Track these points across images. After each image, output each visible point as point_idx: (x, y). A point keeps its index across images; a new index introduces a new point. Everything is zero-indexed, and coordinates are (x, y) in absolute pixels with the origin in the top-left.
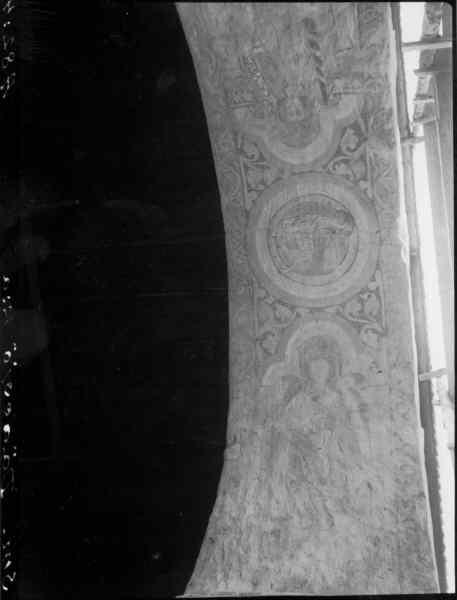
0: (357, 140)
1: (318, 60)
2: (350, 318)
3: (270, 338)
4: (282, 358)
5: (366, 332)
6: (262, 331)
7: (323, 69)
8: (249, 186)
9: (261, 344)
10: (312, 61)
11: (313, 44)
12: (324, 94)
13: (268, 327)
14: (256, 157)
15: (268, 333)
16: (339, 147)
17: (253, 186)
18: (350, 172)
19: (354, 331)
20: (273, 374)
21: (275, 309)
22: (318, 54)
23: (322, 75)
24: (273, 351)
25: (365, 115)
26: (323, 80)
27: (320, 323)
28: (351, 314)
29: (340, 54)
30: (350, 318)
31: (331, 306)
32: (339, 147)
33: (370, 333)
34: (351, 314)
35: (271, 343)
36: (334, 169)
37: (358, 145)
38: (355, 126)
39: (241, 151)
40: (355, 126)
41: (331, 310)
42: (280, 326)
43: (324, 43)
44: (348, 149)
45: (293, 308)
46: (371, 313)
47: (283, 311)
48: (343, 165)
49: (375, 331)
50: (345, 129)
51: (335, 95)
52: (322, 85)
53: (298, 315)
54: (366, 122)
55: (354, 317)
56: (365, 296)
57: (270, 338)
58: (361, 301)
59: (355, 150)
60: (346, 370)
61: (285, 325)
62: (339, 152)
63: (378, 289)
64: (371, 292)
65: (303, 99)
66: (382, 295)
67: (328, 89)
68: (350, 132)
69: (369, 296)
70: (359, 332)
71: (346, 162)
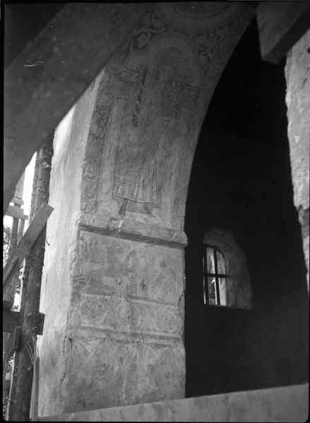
0: (139, 39)
1: (139, 100)
7: (138, 92)
8: (218, 40)
10: (142, 99)
11: (138, 110)
12: (144, 76)
14: (203, 54)
16: (151, 38)
17: (216, 38)
18: (153, 20)
22: (137, 102)
23: (141, 88)
25: (127, 52)
26: (141, 85)
29: (127, 97)
32: (151, 38)
36: (161, 26)
37: (140, 35)
38: (136, 47)
39: (209, 60)
40: (136, 47)
43: (131, 108)
44: (147, 34)
48: (155, 26)
50: (144, 47)
51: (139, 72)
52: (143, 82)
54: (128, 48)
59: (143, 33)
62: (153, 35)
65: (157, 79)
67: (141, 77)
68: (140, 45)
71: (152, 27)
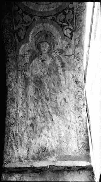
2: (60, 23)
3: (21, 31)
4: (27, 41)
5: (66, 30)
6: (16, 29)
9: (17, 34)
13: (19, 26)
15: (20, 28)
19: (61, 29)
20: (24, 49)
21: (23, 16)
24: (23, 38)
27: (45, 24)
28: (59, 20)
30: (60, 23)
31: (49, 16)
33: (68, 30)
34: (59, 20)
35: (22, 33)
41: (50, 18)
42: (25, 25)
45: (31, 16)
46: (69, 20)
47: (27, 18)
49: (70, 29)
53: (34, 20)
55: (61, 22)
56: (67, 12)
57: (21, 31)
58: (65, 14)
60: (56, 48)
61: (28, 25)
63: (73, 8)
64: (70, 9)
66: (75, 11)
69: (69, 11)
70: (63, 29)
